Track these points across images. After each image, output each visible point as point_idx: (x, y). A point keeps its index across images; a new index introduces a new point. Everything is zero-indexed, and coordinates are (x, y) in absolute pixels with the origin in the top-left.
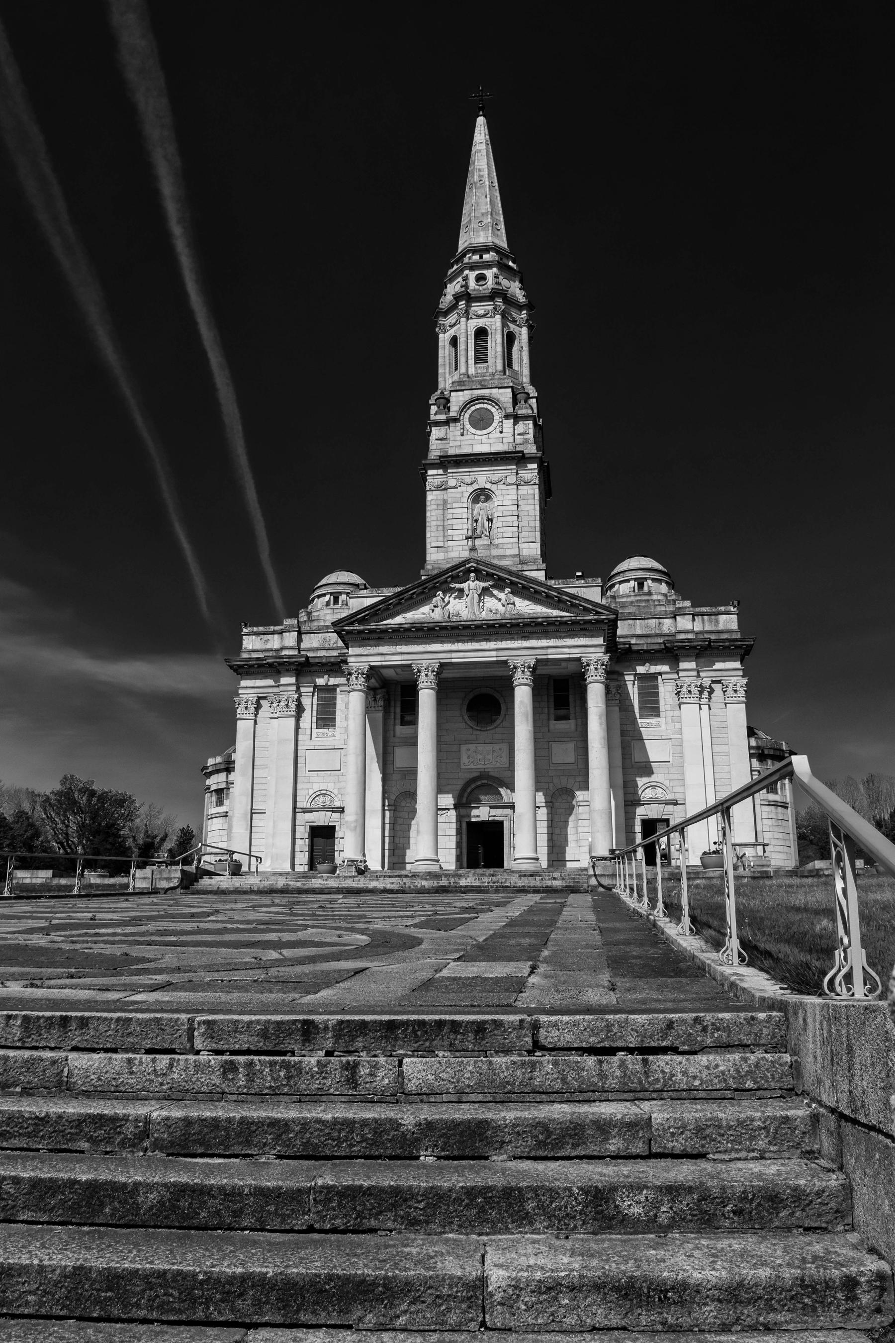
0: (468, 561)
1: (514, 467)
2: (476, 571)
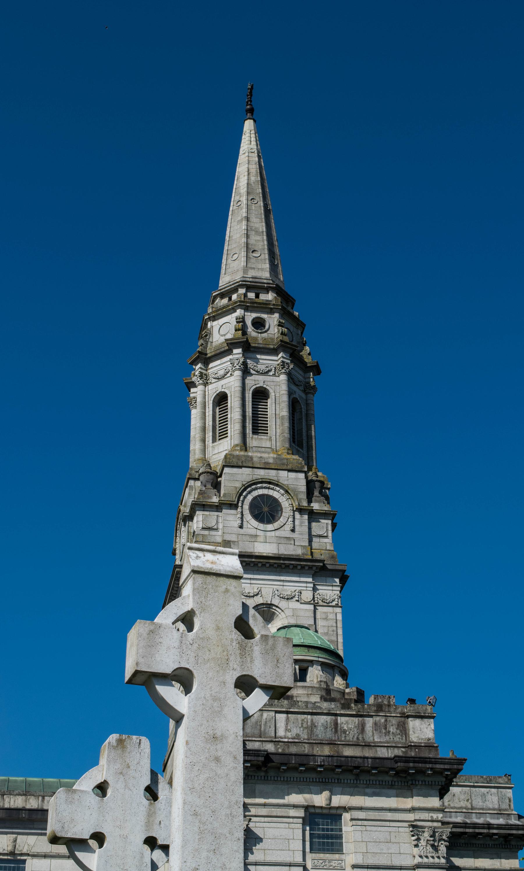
1: (310, 580)
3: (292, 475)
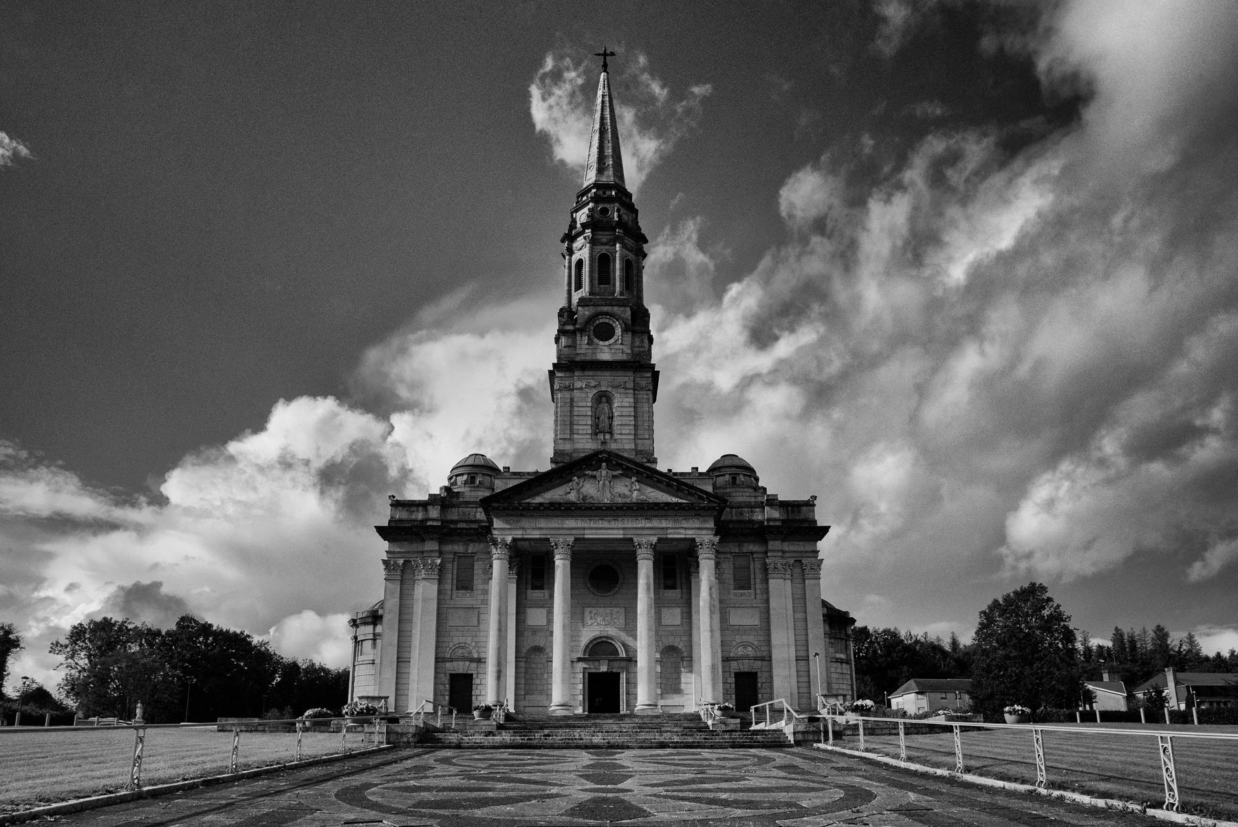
0: (601, 452)
2: (608, 461)
3: (622, 309)
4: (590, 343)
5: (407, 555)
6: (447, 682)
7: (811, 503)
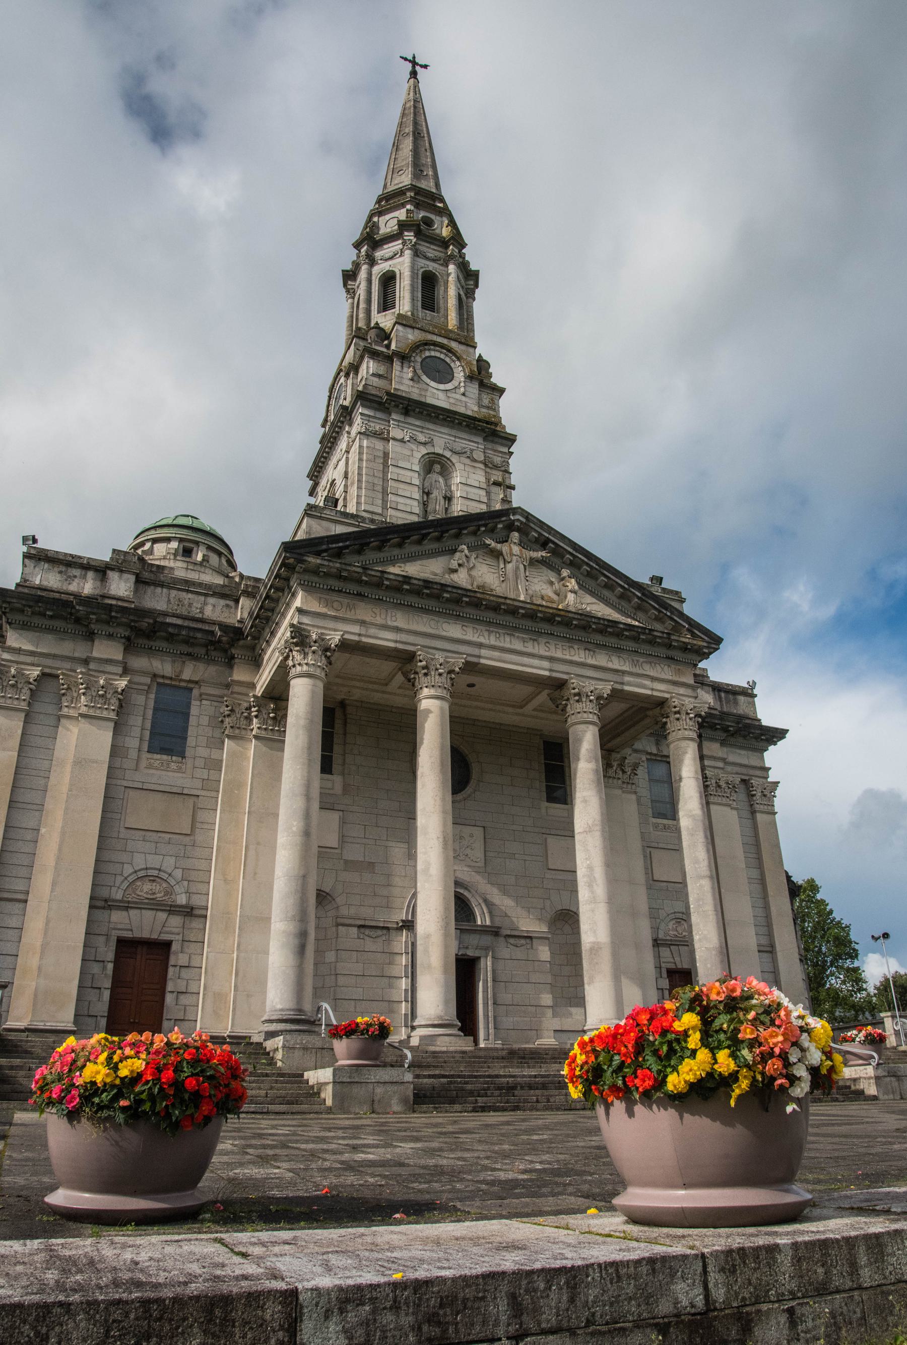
3: (463, 347)
4: (415, 379)
5: (49, 662)
6: (111, 956)
7: (750, 691)
